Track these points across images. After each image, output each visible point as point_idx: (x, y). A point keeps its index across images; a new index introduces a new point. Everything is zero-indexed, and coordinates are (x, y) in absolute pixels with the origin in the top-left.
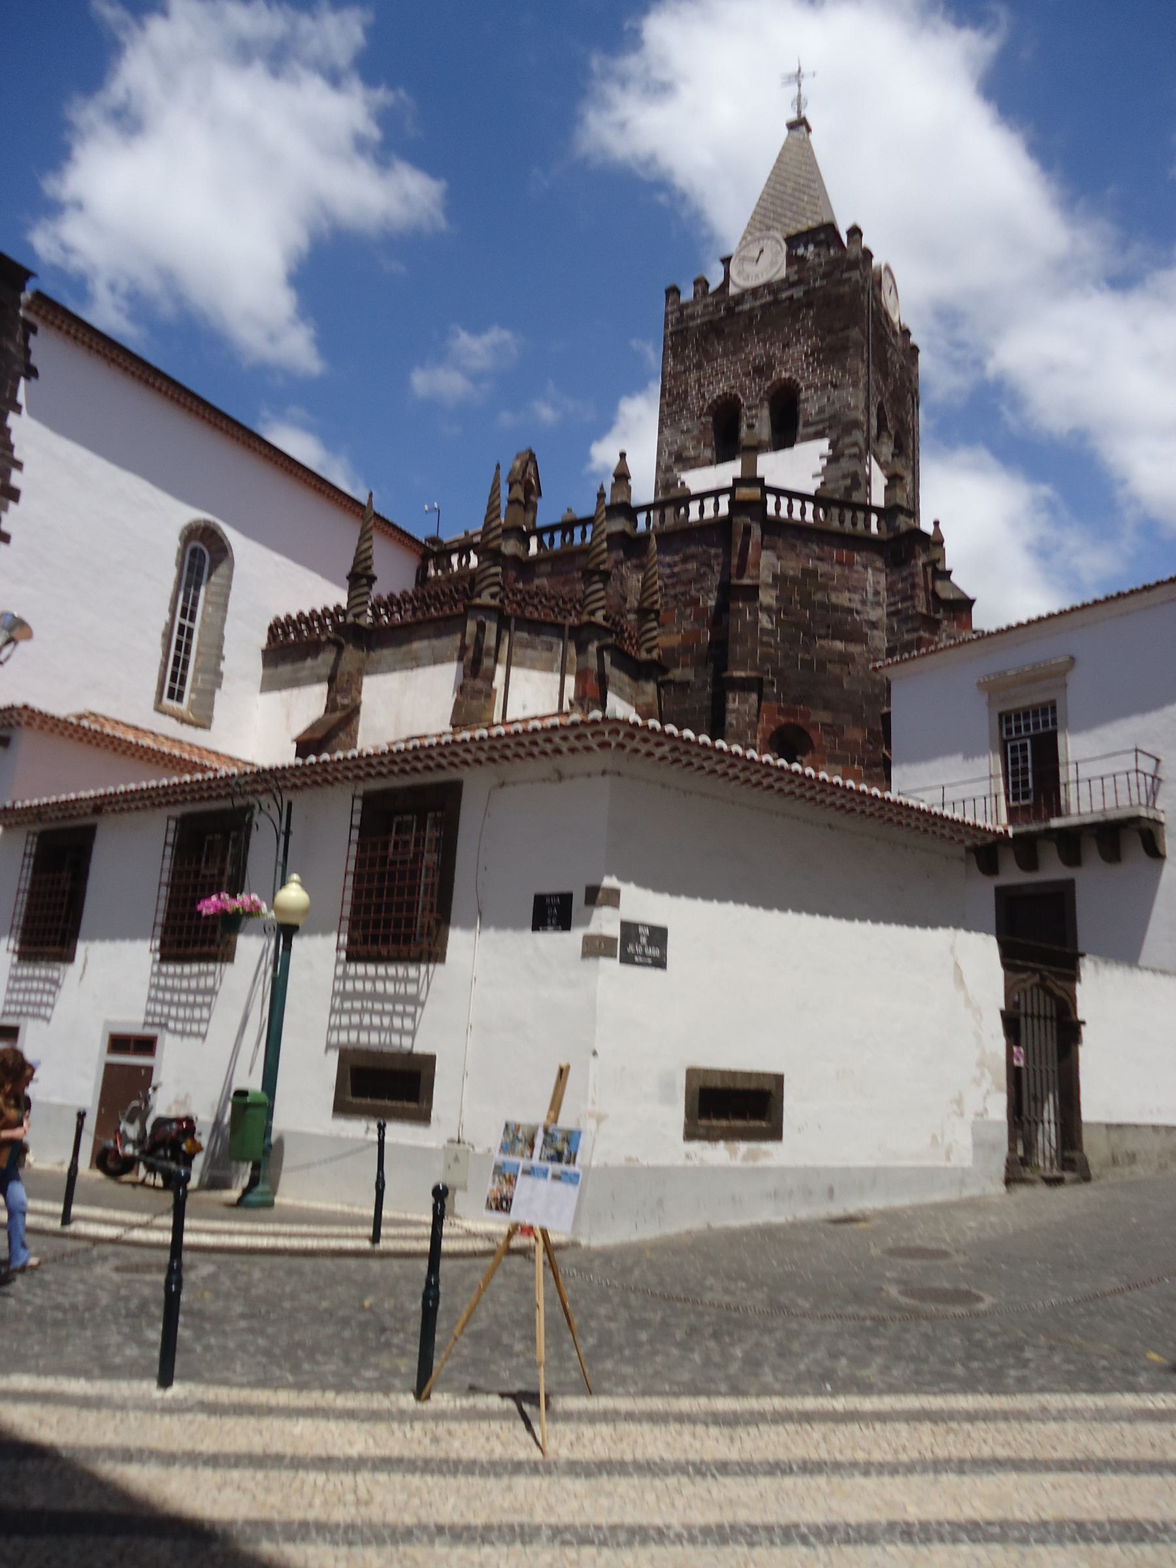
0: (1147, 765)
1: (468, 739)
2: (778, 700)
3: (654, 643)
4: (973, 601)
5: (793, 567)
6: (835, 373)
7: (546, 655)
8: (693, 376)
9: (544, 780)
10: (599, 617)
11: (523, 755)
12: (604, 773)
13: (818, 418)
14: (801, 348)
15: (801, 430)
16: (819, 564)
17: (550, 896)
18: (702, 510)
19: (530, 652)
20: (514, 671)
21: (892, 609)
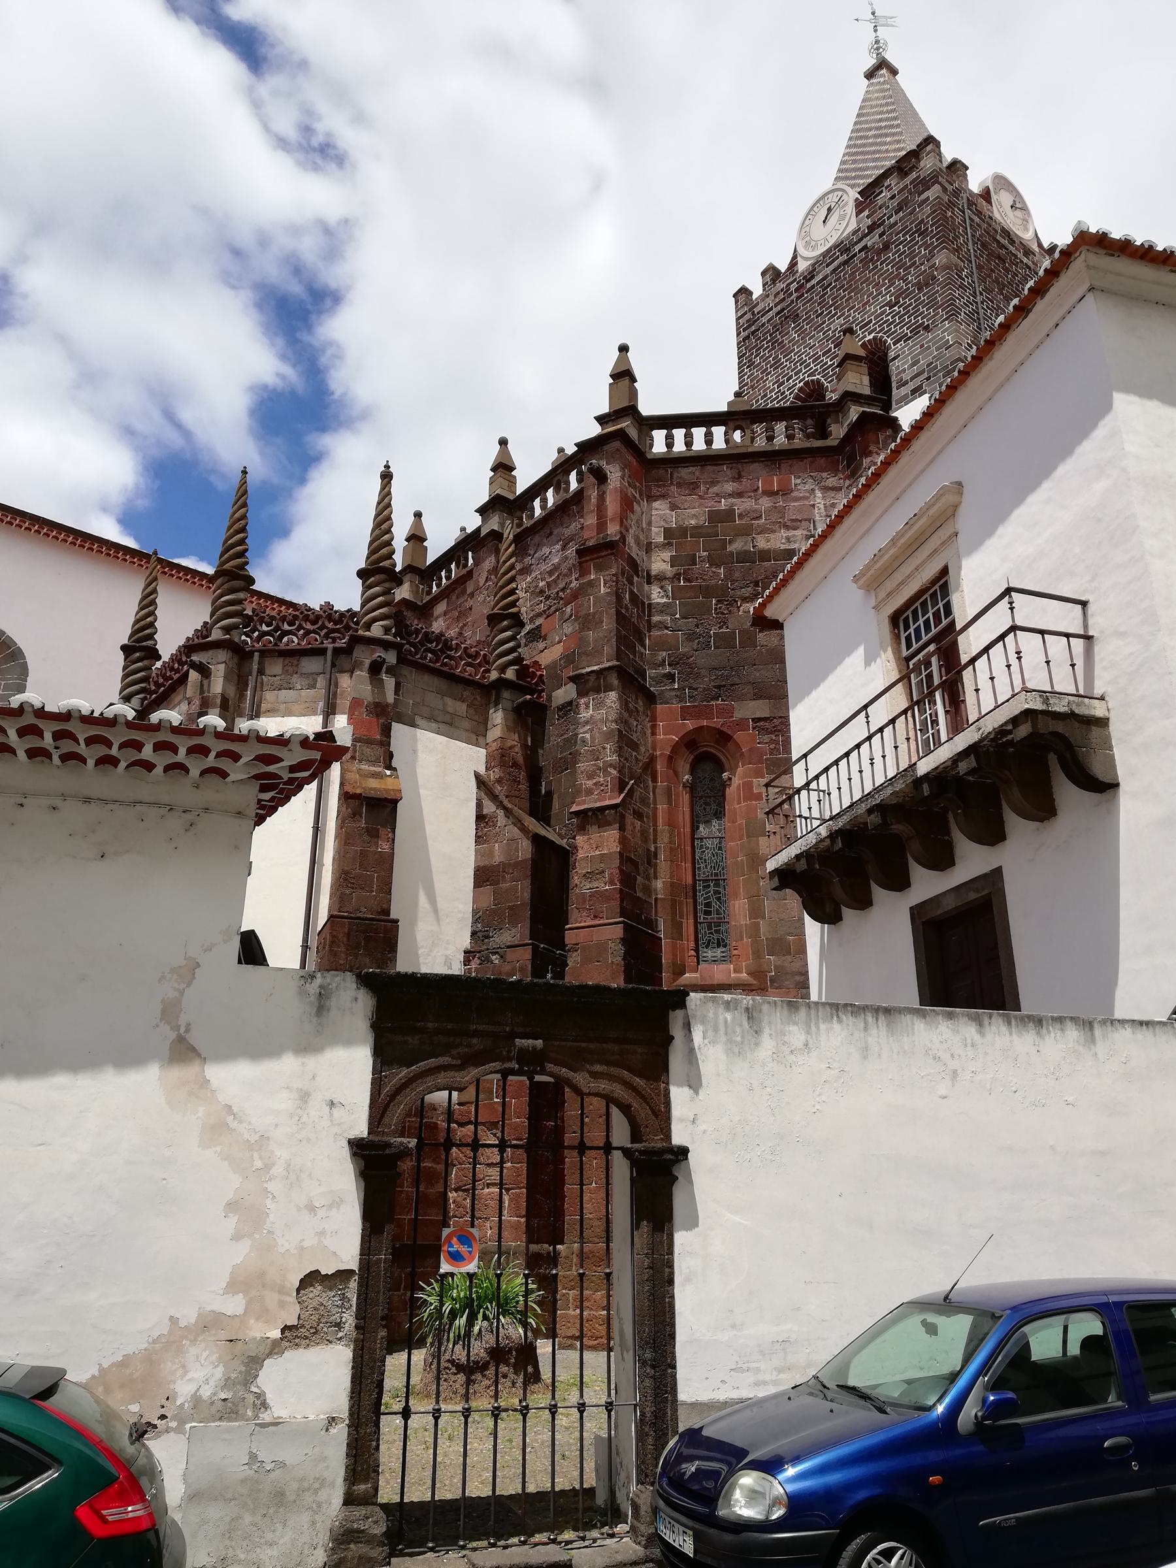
2: (681, 699)
5: (694, 514)
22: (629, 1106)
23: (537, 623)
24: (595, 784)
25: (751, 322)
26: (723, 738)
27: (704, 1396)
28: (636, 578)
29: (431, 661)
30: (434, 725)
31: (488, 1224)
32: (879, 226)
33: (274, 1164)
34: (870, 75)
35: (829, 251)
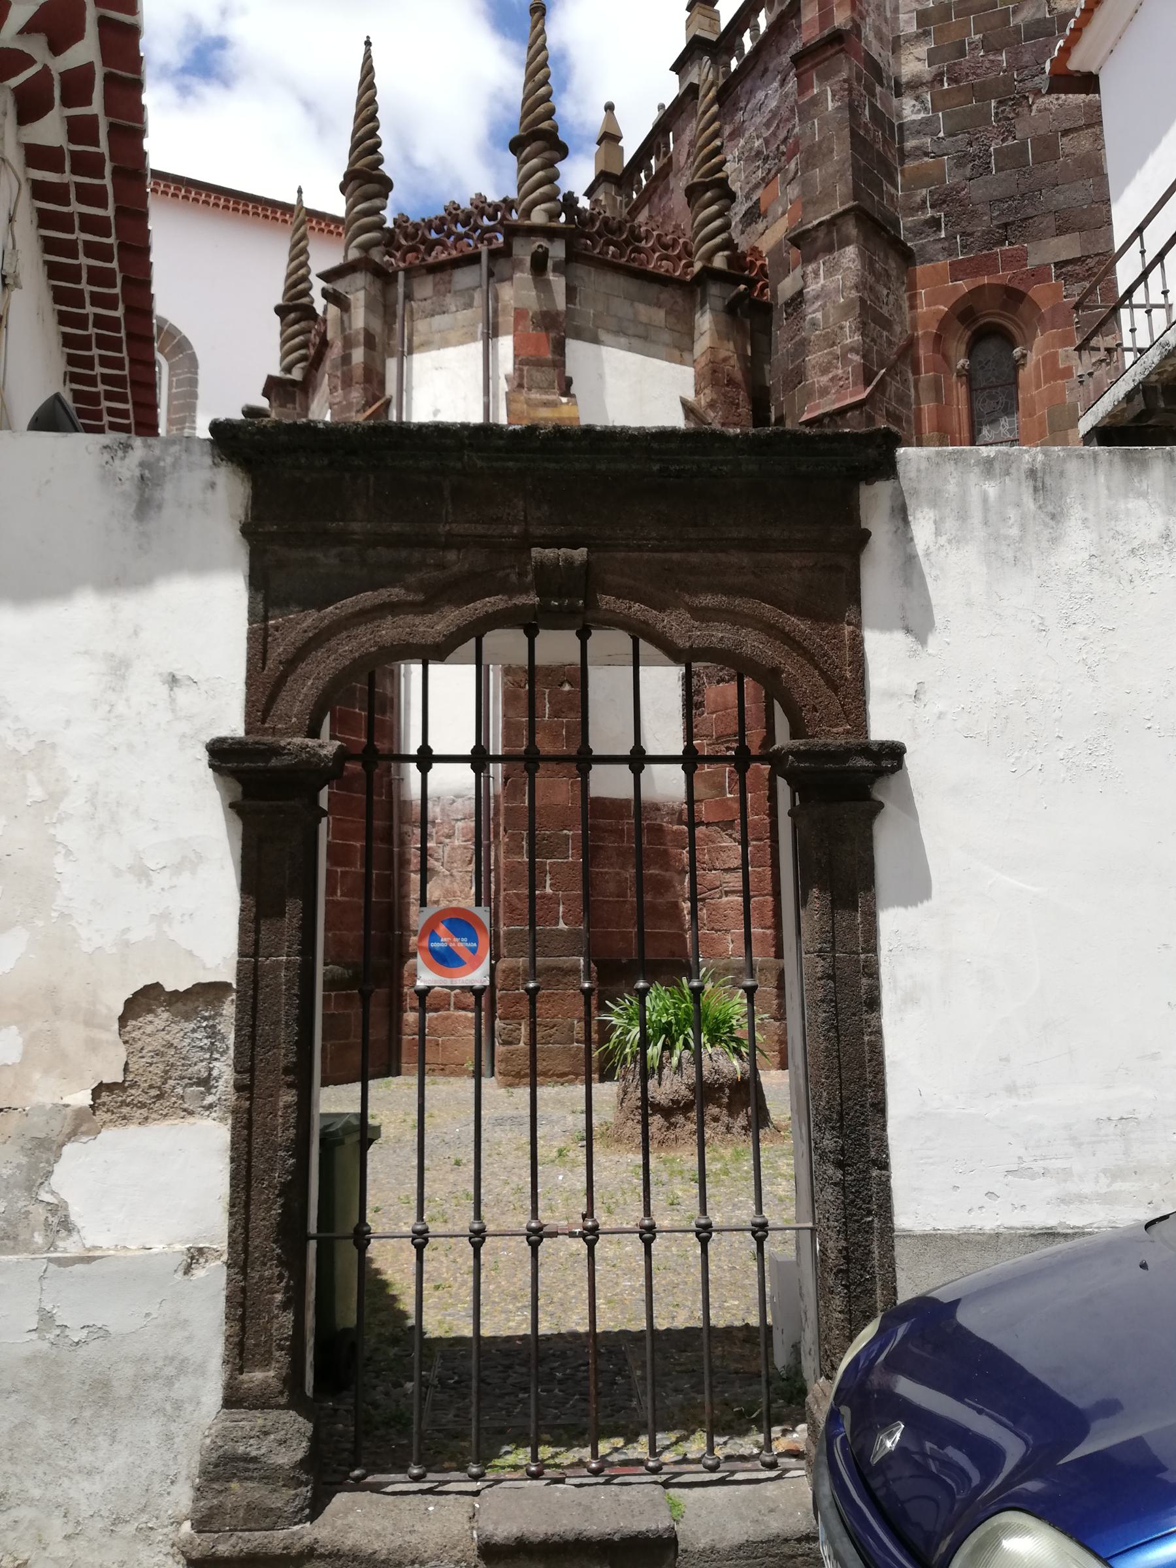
2: (951, 252)
19: (439, 321)
22: (776, 672)
23: (755, 198)
24: (832, 380)
26: (1013, 297)
27: (950, 1221)
28: (878, 89)
29: (613, 256)
30: (623, 340)
31: (729, 937)
33: (66, 792)
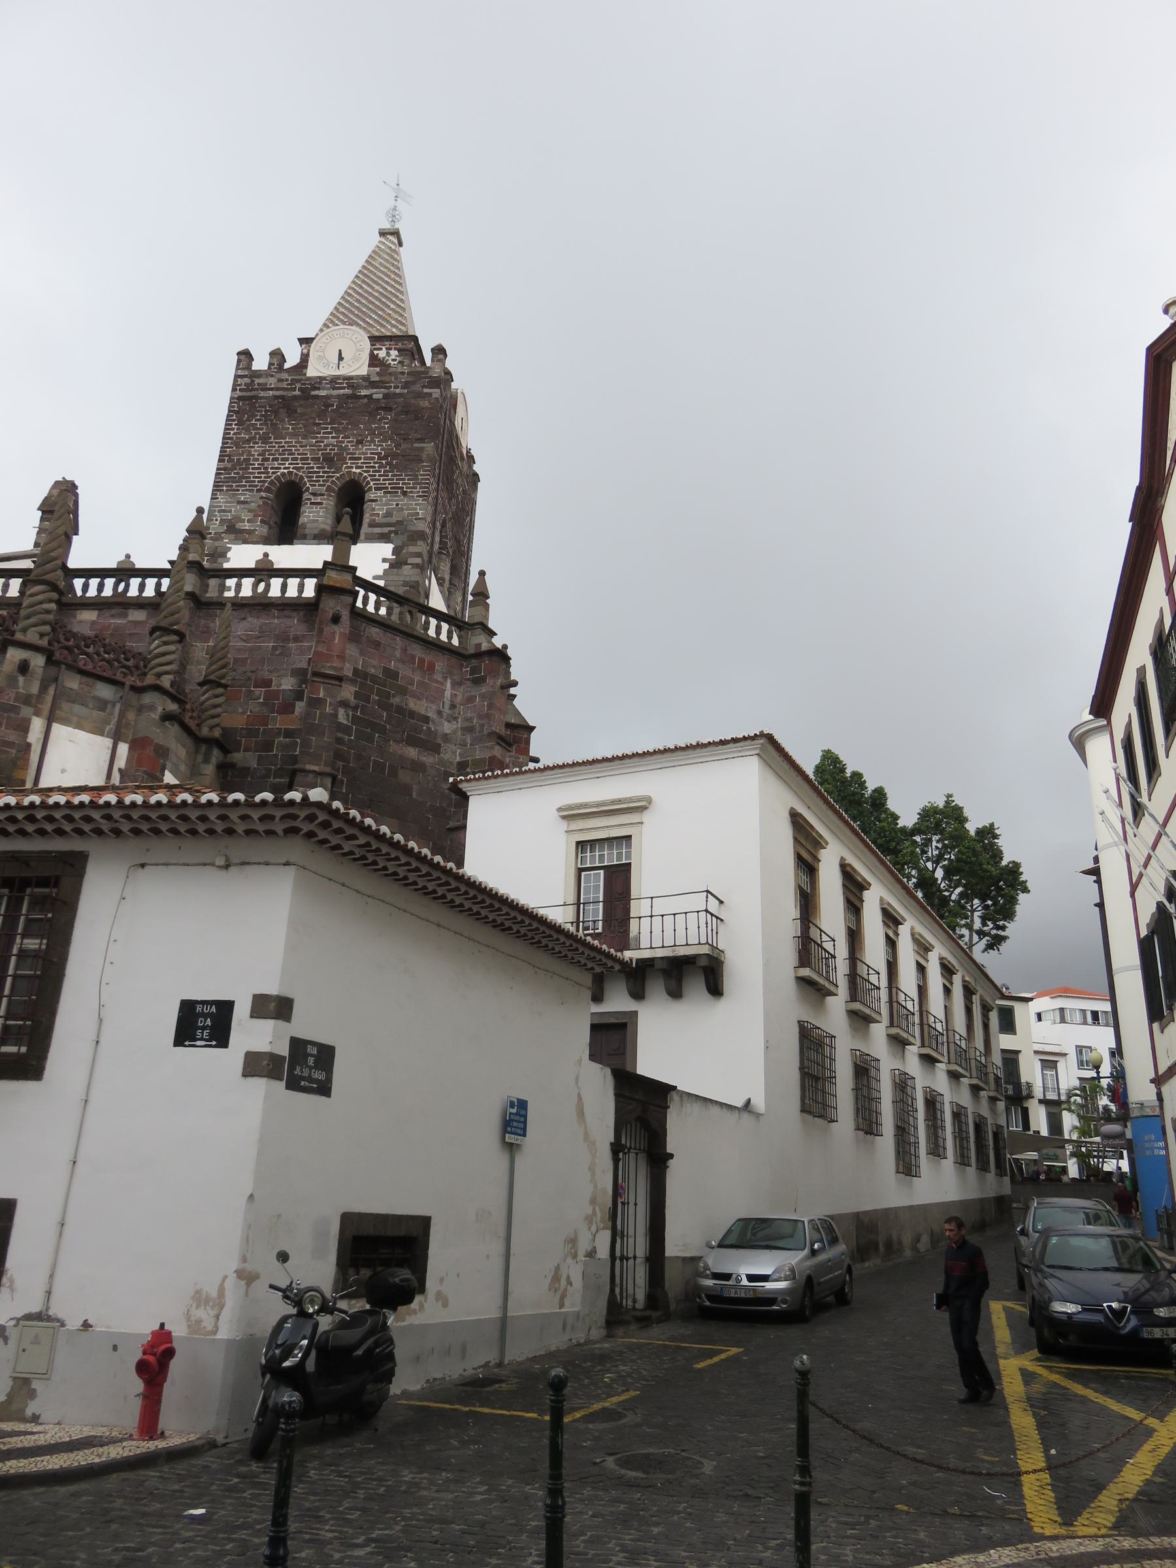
0: (713, 905)
1: (62, 803)
3: (217, 720)
4: (533, 728)
6: (406, 482)
7: (96, 713)
8: (257, 449)
9: (205, 865)
10: (166, 682)
11: (182, 831)
12: (287, 864)
13: (385, 520)
14: (374, 448)
15: (365, 529)
16: (400, 665)
17: (203, 1002)
18: (284, 587)
20: (56, 727)
21: (467, 724)
25: (249, 387)
27: (673, 1255)
32: (385, 388)
34: (383, 233)
35: (338, 377)
